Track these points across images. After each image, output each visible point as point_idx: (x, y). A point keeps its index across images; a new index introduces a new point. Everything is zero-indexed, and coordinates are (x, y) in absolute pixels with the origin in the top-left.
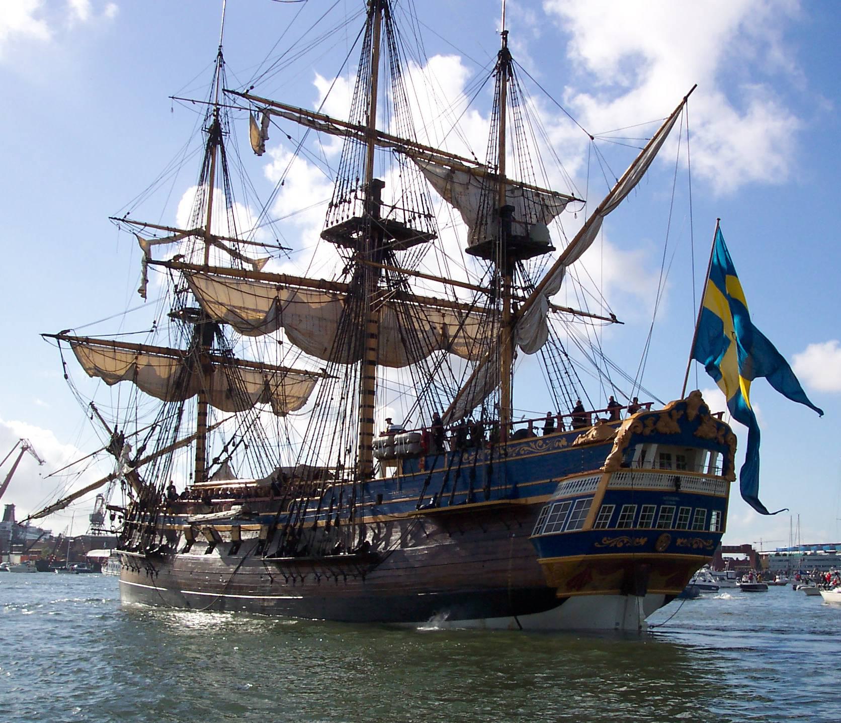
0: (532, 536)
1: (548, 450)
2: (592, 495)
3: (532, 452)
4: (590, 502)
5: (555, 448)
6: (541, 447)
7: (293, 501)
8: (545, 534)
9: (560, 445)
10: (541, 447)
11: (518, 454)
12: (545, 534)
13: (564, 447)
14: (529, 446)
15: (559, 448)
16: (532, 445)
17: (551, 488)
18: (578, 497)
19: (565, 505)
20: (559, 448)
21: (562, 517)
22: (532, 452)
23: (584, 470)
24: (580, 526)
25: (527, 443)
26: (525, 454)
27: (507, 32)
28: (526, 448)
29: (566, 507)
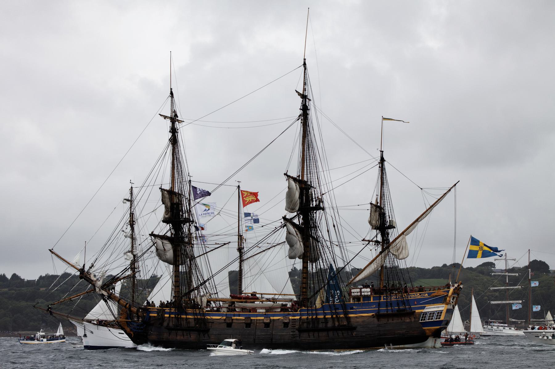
0: (420, 321)
1: (421, 297)
2: (443, 310)
3: (415, 297)
4: (441, 313)
5: (423, 296)
6: (419, 296)
7: (300, 309)
8: (428, 321)
9: (426, 295)
10: (419, 296)
11: (411, 297)
12: (421, 321)
13: (427, 296)
14: (414, 295)
15: (425, 296)
16: (416, 295)
17: (423, 308)
18: (437, 311)
19: (433, 313)
20: (425, 296)
21: (433, 316)
22: (415, 297)
23: (438, 303)
24: (439, 318)
25: (414, 294)
26: (413, 297)
27: (383, 152)
28: (413, 296)
29: (434, 313)
